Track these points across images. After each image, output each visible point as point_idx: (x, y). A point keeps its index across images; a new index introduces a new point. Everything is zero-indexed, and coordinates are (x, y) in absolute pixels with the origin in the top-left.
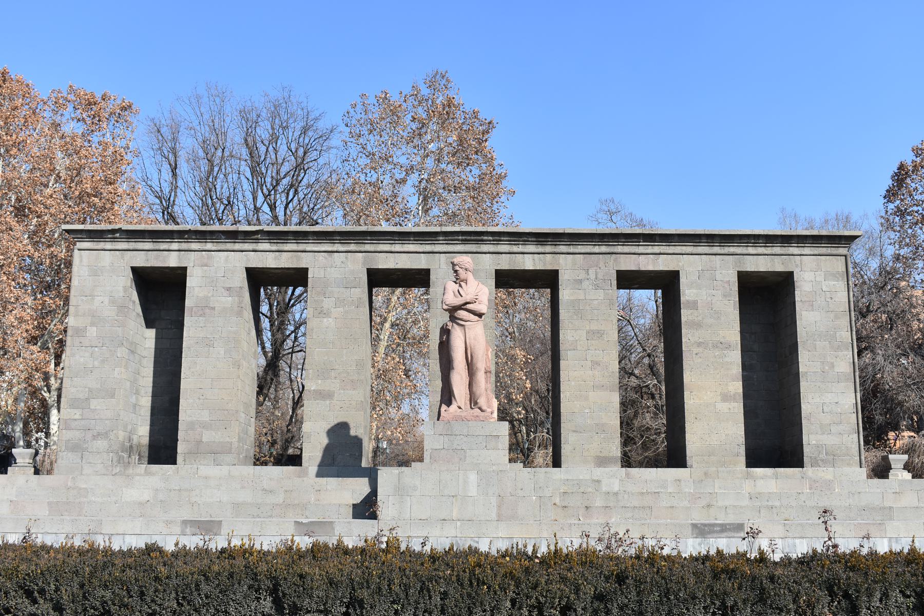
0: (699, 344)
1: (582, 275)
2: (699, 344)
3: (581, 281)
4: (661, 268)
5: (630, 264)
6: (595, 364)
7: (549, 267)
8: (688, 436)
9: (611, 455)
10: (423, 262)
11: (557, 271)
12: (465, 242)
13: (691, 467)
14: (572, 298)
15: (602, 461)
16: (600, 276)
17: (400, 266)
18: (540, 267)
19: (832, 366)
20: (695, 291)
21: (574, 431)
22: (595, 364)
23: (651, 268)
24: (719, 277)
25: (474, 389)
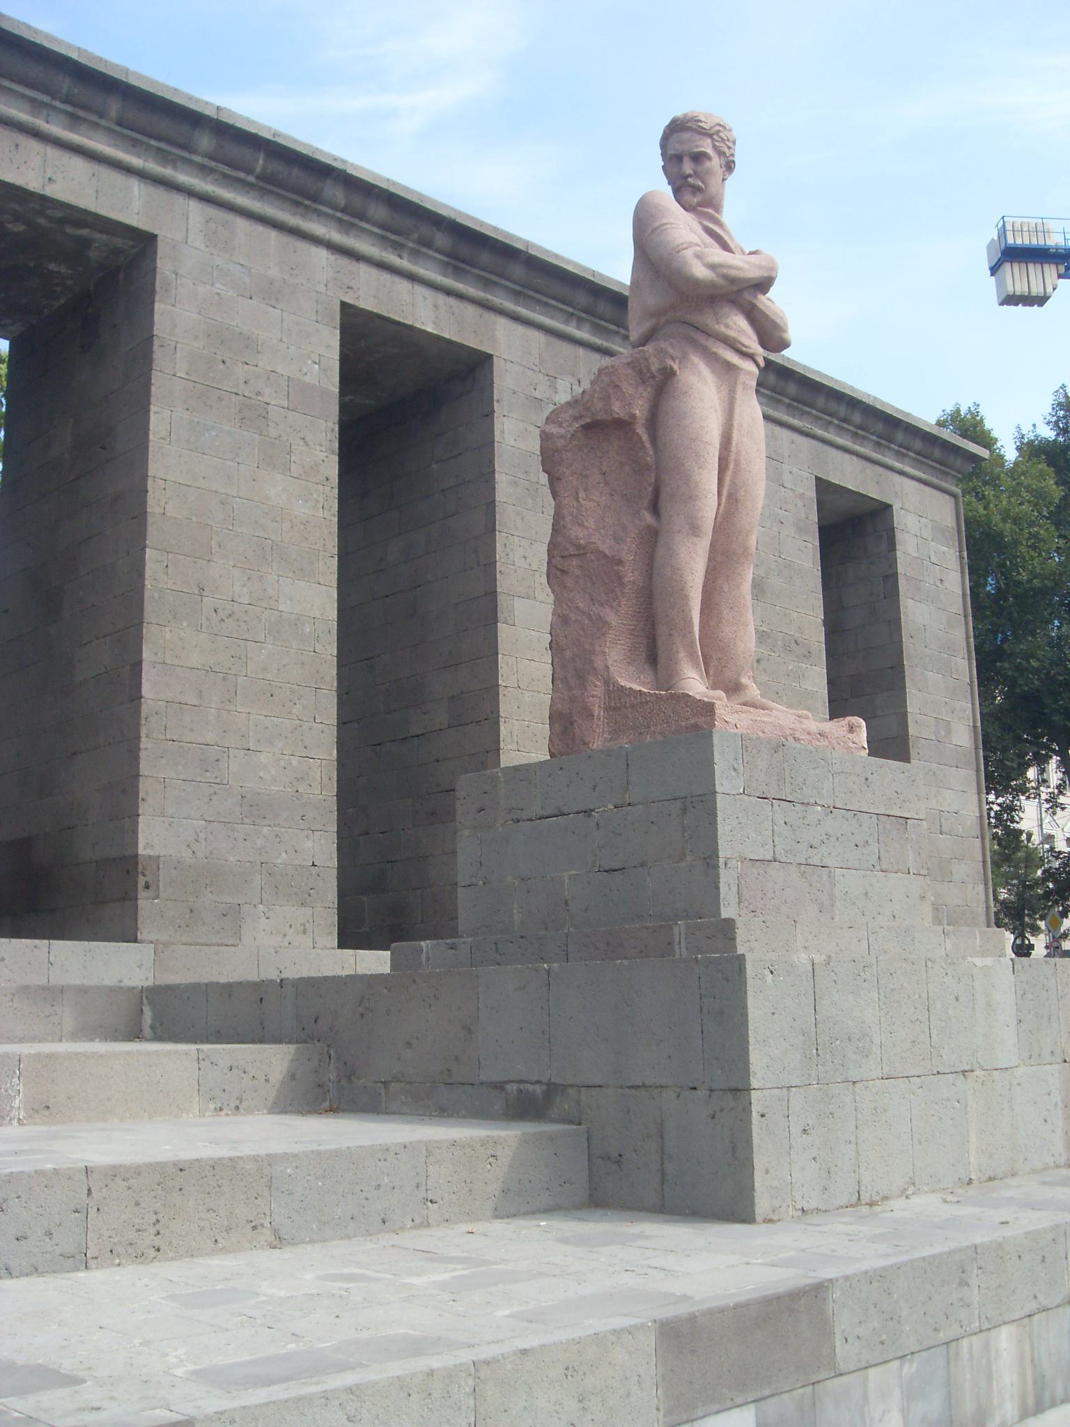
7: (473, 343)
10: (137, 204)
11: (489, 357)
12: (269, 185)
17: (56, 191)
18: (449, 333)
19: (949, 732)
24: (787, 479)
25: (727, 631)
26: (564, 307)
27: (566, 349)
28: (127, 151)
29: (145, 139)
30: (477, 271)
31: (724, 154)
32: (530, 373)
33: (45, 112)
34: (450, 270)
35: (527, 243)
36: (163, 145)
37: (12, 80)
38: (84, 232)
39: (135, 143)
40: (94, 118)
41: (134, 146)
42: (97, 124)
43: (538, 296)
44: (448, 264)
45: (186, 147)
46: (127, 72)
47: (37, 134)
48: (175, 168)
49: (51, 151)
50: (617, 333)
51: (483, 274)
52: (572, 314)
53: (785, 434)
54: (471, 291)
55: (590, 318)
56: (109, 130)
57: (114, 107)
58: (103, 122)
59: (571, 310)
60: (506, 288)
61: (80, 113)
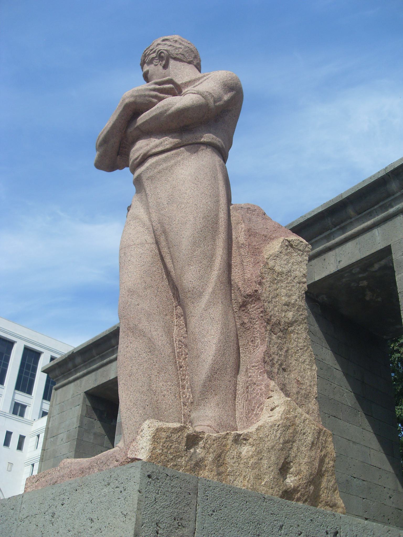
28: (369, 220)
29: (372, 209)
31: (153, 59)
33: (332, 237)
36: (381, 204)
37: (315, 238)
38: (376, 266)
39: (370, 215)
40: (349, 221)
41: (371, 215)
42: (351, 222)
45: (389, 196)
46: (341, 195)
47: (330, 249)
48: (392, 207)
49: (337, 250)
56: (357, 220)
57: (350, 211)
58: (353, 219)
61: (343, 225)
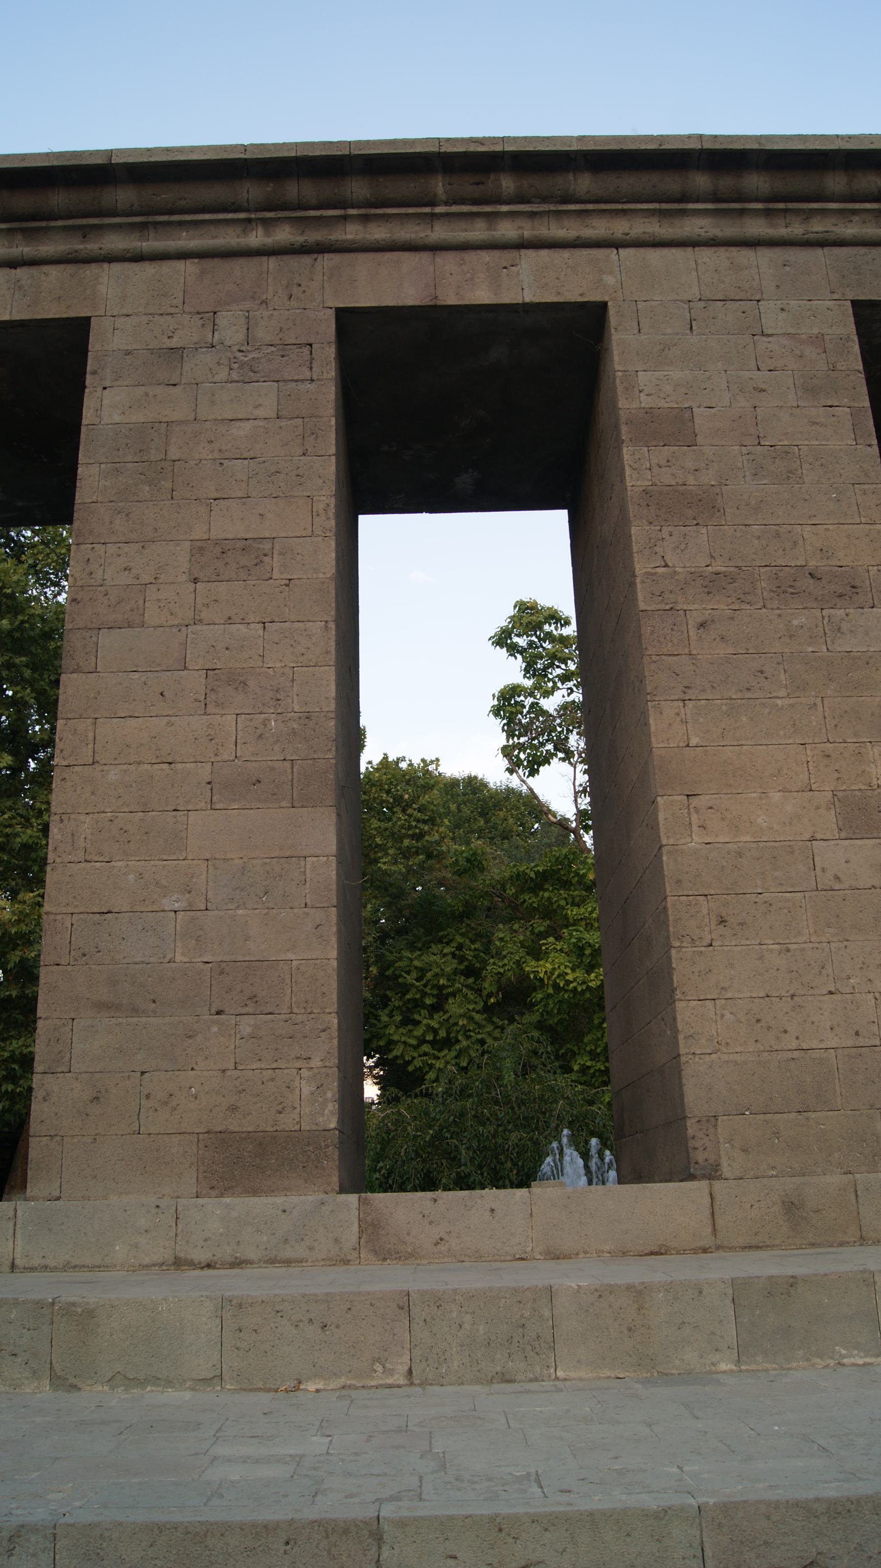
0: (713, 584)
1: (188, 333)
2: (713, 584)
3: (177, 354)
4: (529, 297)
5: (394, 283)
6: (223, 680)
8: (686, 1012)
9: (288, 1122)
13: (712, 1173)
14: (137, 417)
15: (241, 1160)
16: (262, 333)
20: (677, 375)
21: (103, 1006)
22: (223, 680)
23: (482, 295)
26: (230, 216)
27: (240, 268)
30: (60, 223)
32: (162, 320)
34: (19, 237)
35: (110, 153)
43: (176, 218)
44: (10, 231)
50: (345, 218)
51: (70, 222)
52: (249, 221)
53: (764, 258)
54: (47, 249)
55: (281, 214)
59: (242, 216)
60: (119, 226)
